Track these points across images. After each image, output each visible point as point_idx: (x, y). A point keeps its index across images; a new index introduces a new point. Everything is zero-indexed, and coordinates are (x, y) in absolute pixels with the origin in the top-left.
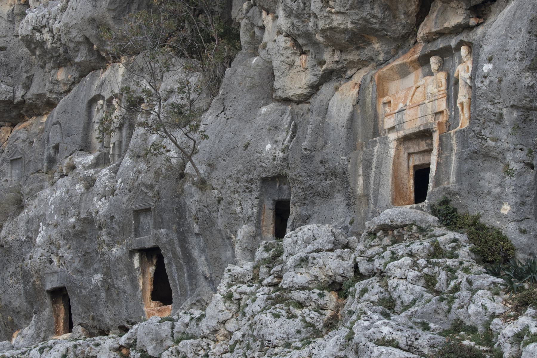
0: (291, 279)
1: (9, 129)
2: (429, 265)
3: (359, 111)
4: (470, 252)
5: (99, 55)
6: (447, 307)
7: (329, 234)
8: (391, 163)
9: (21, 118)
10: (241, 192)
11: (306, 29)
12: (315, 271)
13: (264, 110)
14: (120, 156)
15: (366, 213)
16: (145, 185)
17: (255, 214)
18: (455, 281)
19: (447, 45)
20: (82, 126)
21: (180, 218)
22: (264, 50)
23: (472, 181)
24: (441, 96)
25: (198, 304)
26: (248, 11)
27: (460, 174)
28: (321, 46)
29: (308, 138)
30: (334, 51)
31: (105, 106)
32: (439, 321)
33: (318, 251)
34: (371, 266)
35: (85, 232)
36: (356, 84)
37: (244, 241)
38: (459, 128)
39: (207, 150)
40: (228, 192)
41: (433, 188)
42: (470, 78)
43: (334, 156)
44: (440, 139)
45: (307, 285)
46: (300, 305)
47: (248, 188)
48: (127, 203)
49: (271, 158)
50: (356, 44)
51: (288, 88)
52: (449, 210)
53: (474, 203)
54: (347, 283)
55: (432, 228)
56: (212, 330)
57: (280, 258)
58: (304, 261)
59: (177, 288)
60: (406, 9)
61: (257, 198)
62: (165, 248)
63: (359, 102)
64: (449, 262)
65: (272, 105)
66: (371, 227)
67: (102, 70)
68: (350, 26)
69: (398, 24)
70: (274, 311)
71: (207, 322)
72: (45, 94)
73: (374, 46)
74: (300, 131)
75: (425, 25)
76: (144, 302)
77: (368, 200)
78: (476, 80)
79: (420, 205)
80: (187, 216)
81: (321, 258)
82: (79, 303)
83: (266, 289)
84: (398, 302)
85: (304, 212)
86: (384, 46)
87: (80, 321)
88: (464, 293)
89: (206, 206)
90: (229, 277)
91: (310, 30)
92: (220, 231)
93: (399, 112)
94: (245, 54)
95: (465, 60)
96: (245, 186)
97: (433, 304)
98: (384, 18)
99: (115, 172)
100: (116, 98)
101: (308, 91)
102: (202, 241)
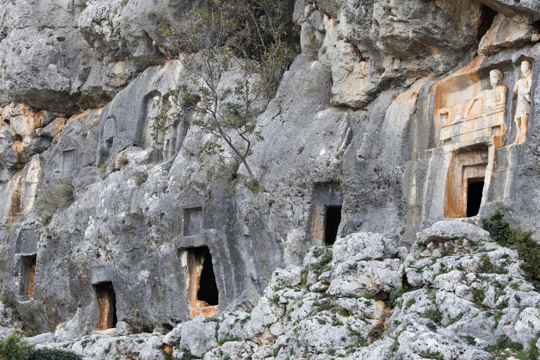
0: (339, 286)
1: (63, 120)
2: (478, 280)
3: (416, 121)
4: (519, 269)
5: (158, 50)
6: (493, 323)
7: (379, 243)
8: (446, 175)
9: (75, 110)
10: (293, 196)
11: (367, 35)
12: (363, 279)
13: (320, 114)
14: (173, 153)
15: (417, 224)
16: (197, 183)
17: (306, 219)
18: (503, 296)
19: (507, 59)
20: (136, 121)
21: (230, 219)
22: (324, 55)
23: (526, 198)
24: (499, 110)
25: (244, 306)
26: (309, 15)
27: (514, 190)
28: (381, 53)
29: (363, 146)
30: (393, 59)
31: (161, 103)
32: (484, 337)
33: (367, 259)
34: (419, 277)
35: (135, 228)
36: (414, 93)
37: (294, 245)
38: (515, 143)
39: (262, 152)
40: (280, 195)
41: (486, 202)
42: (530, 94)
43: (388, 165)
44: (496, 153)
45: (354, 293)
46: (346, 313)
47: (300, 192)
48: (178, 201)
49: (325, 163)
50: (416, 53)
51: (346, 94)
52: (500, 225)
53: (526, 220)
54: (395, 293)
55: (483, 242)
56: (257, 332)
57: (329, 264)
58: (353, 268)
59: (223, 289)
60: (468, 21)
61: (308, 203)
62: (213, 248)
63: (416, 112)
64: (499, 277)
65: (329, 111)
66: (422, 238)
67: (160, 66)
68: (411, 35)
69: (460, 36)
70: (320, 318)
71: (252, 324)
72: (101, 87)
73: (434, 57)
74: (355, 138)
75: (487, 38)
76: (190, 301)
77: (420, 210)
78: (535, 96)
79: (472, 218)
80: (238, 217)
81: (371, 267)
82: (124, 299)
83: (313, 295)
84: (445, 315)
85: (355, 220)
87: (125, 316)
88: (511, 310)
89: (257, 208)
90: (277, 281)
91: (371, 36)
92: (269, 234)
93: (456, 124)
94: (304, 58)
95: (525, 75)
96: (297, 190)
97: (480, 319)
98: (446, 29)
99: (168, 169)
100: (173, 94)
101: (365, 97)
102: (251, 243)
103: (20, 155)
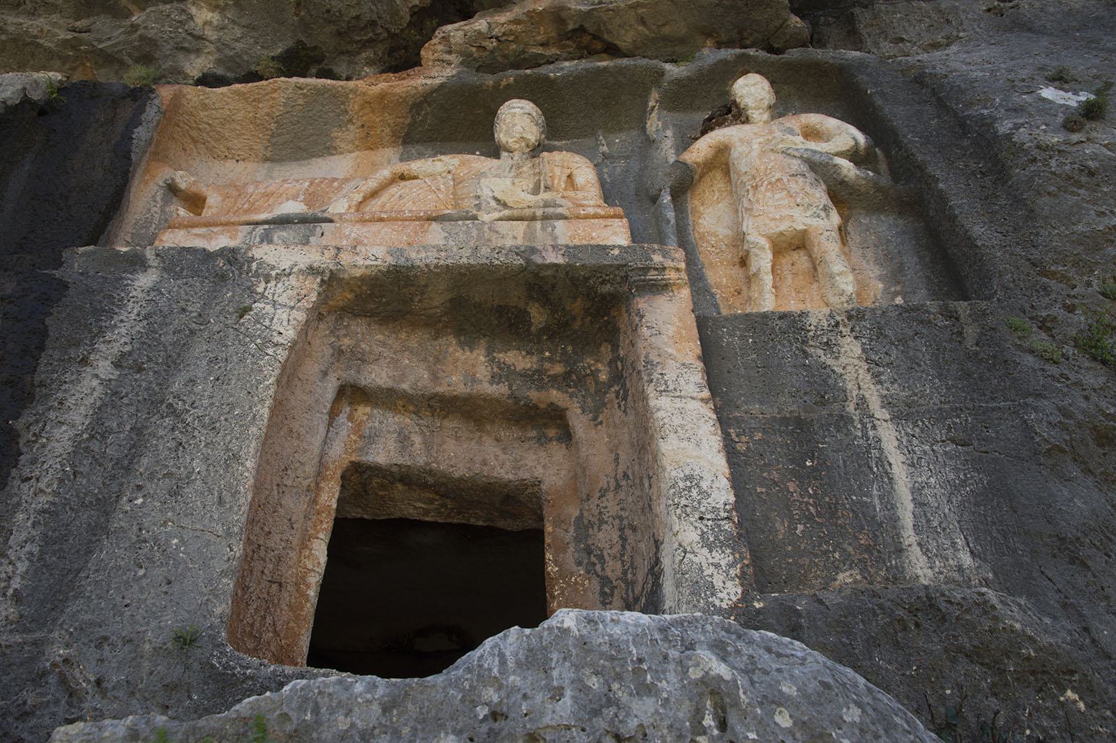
24: (591, 211)
86: (238, 32)
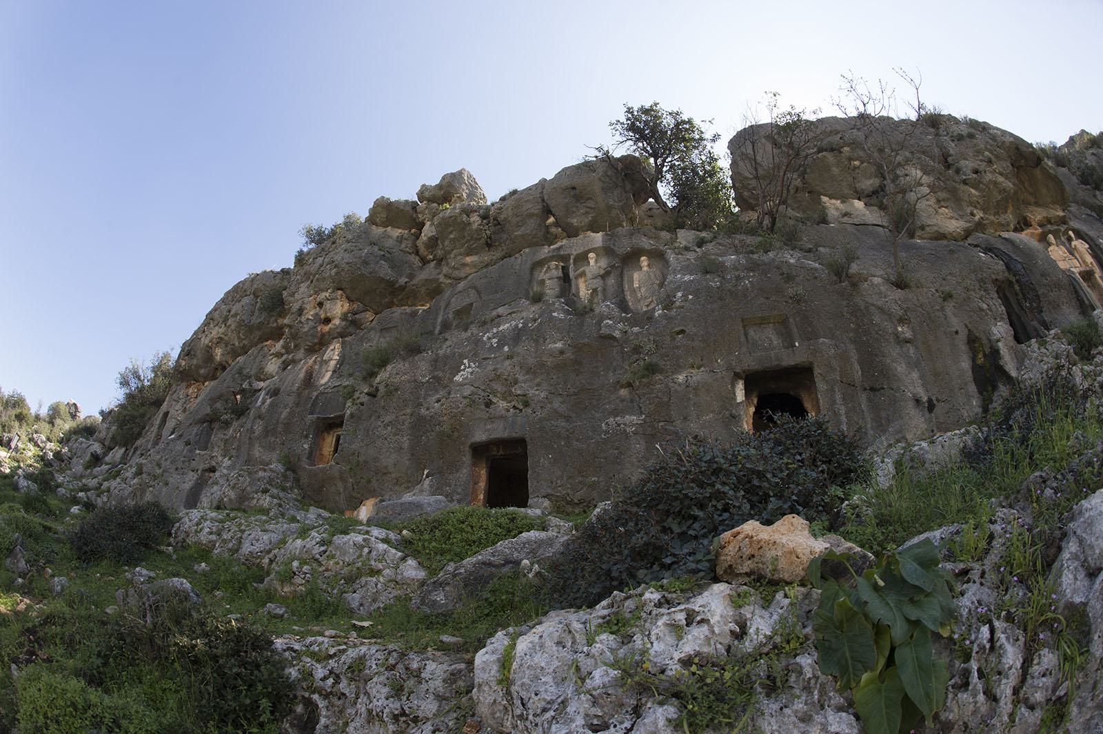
103: (323, 335)
